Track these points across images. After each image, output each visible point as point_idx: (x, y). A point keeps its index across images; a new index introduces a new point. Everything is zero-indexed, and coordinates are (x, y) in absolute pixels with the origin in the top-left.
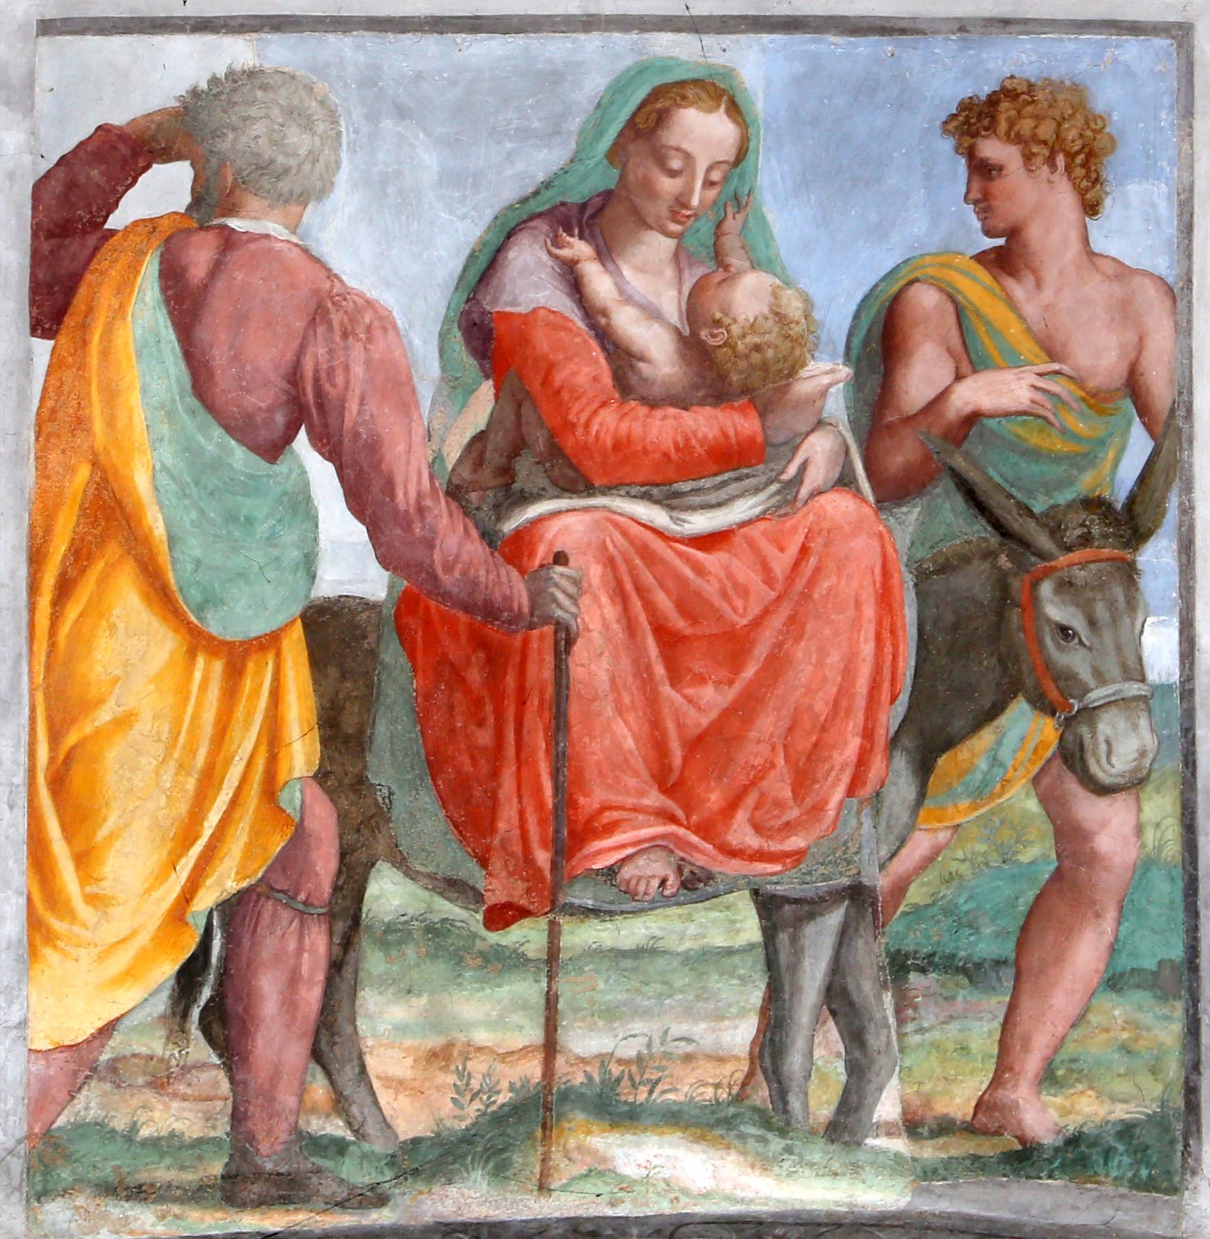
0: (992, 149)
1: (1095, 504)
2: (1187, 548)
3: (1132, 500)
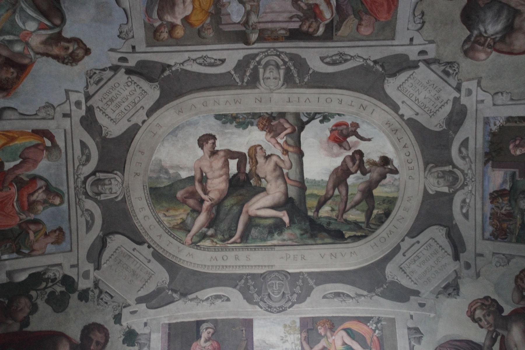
0: (57, 232)
1: (20, 248)
2: (17, 258)
3: (21, 252)
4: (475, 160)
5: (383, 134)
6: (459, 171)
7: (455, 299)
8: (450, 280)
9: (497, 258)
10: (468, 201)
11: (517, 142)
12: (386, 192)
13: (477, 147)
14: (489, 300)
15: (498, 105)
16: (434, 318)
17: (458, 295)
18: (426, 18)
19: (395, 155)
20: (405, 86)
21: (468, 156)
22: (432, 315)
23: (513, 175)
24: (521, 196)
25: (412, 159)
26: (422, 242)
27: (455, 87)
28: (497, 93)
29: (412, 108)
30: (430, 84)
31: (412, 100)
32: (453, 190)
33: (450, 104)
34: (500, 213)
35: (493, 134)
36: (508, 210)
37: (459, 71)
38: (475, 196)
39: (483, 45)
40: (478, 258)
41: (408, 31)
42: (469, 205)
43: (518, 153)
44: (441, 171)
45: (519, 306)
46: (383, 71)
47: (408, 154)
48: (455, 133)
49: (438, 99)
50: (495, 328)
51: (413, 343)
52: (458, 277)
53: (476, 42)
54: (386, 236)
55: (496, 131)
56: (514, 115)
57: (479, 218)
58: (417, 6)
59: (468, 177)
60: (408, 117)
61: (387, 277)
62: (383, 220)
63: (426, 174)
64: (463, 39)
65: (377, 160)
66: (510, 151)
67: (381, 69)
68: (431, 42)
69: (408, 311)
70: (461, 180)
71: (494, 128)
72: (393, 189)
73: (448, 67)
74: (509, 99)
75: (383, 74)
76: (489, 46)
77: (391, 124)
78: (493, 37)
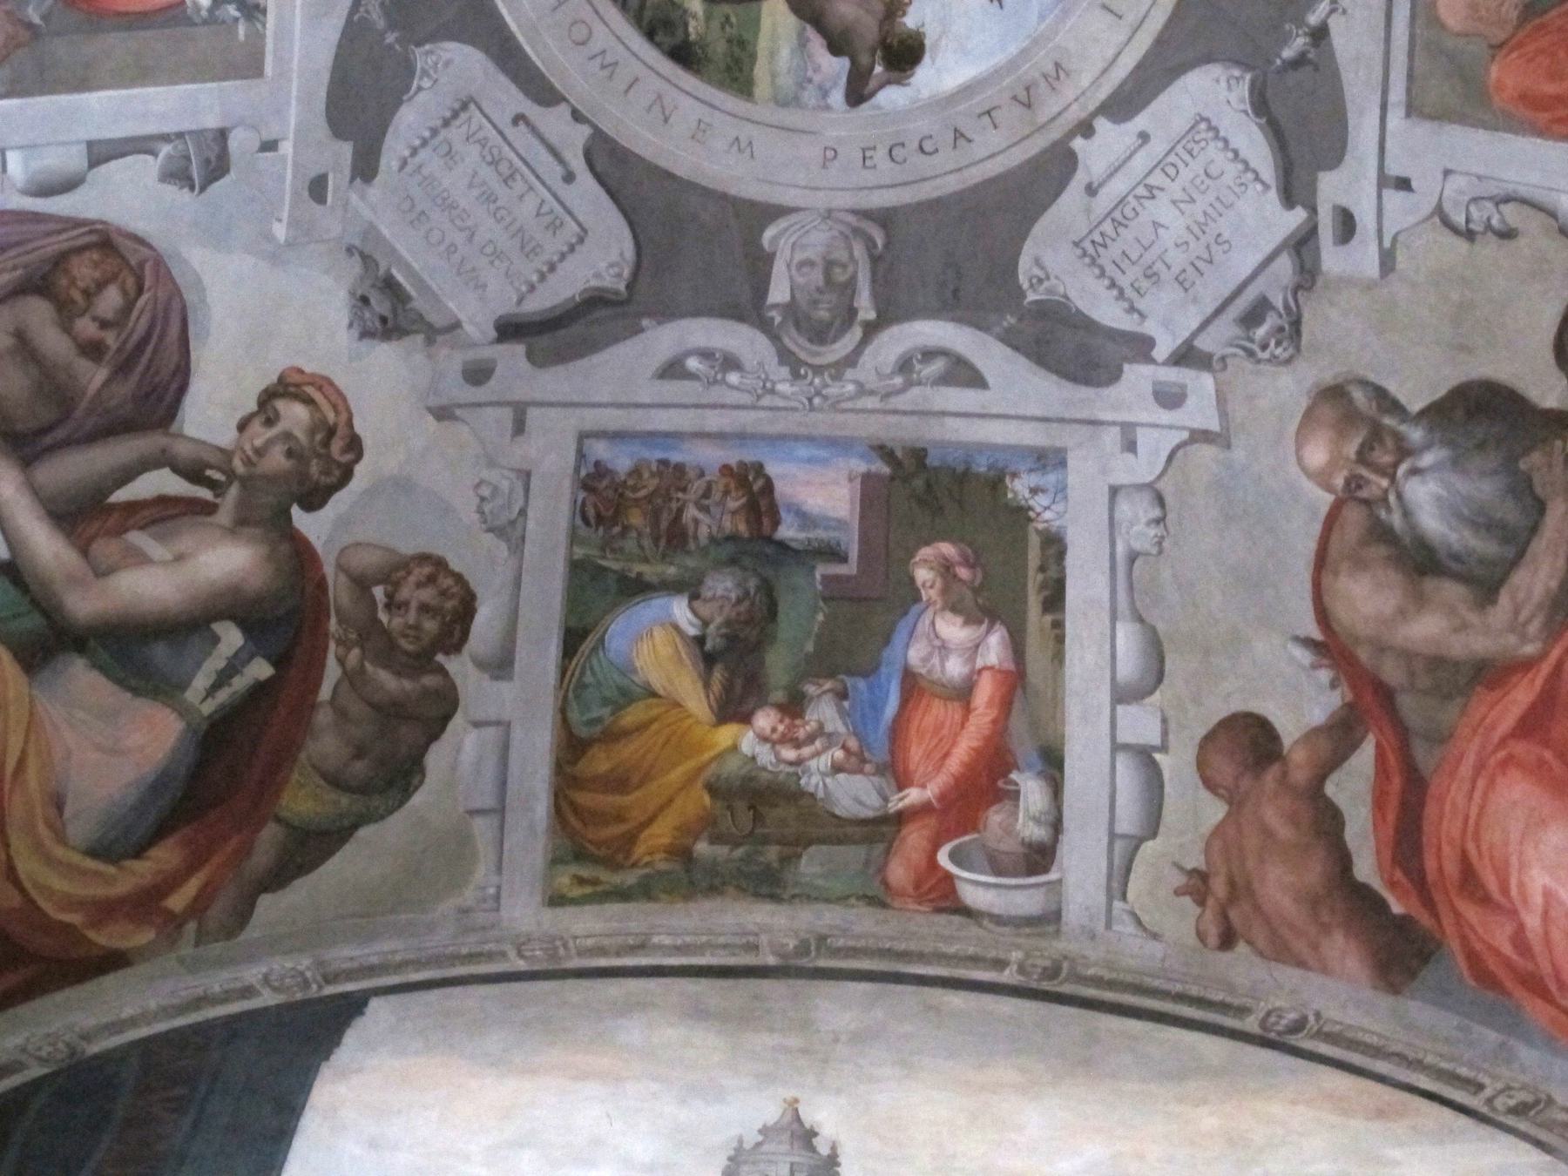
4: (895, 412)
5: (1013, 49)
6: (850, 348)
7: (346, 321)
8: (419, 303)
9: (511, 491)
10: (733, 378)
11: (963, 573)
12: (773, 54)
13: (950, 422)
14: (349, 457)
15: (1111, 510)
16: (269, 237)
17: (365, 334)
18: (1488, 249)
19: (925, 94)
20: (1213, 150)
21: (909, 384)
22: (280, 231)
23: (834, 554)
24: (752, 583)
25: (905, 161)
26: (570, 194)
27: (1199, 343)
28: (1160, 500)
29: (1117, 170)
30: (1214, 248)
31: (1150, 172)
32: (778, 319)
33: (1125, 323)
34: (685, 502)
35: (996, 483)
36: (696, 529)
37: (1259, 361)
38: (754, 407)
39: (1362, 457)
40: (507, 414)
41: (1440, 177)
42: (715, 382)
43: (922, 575)
44: (854, 278)
45: (329, 570)
46: (1278, 62)
47: (928, 146)
48: (1010, 339)
49: (1151, 275)
50: (245, 482)
51: (165, 149)
52: (432, 333)
53: (1376, 434)
54: (596, 46)
55: (1010, 495)
56: (1070, 560)
57: (663, 421)
58: (1542, 215)
59: (829, 381)
60: (1080, 157)
61: (427, 47)
62: (657, 39)
63: (842, 216)
64: (1392, 387)
65: (910, 21)
66: (927, 543)
67: (1288, 53)
68: (1387, 261)
69: (291, 136)
70: (817, 354)
71: (1019, 488)
72: (786, 82)
73: (1279, 322)
74: (1137, 545)
75: (1270, 62)
76: (1354, 483)
77: (1055, 84)
78: (1392, 498)
